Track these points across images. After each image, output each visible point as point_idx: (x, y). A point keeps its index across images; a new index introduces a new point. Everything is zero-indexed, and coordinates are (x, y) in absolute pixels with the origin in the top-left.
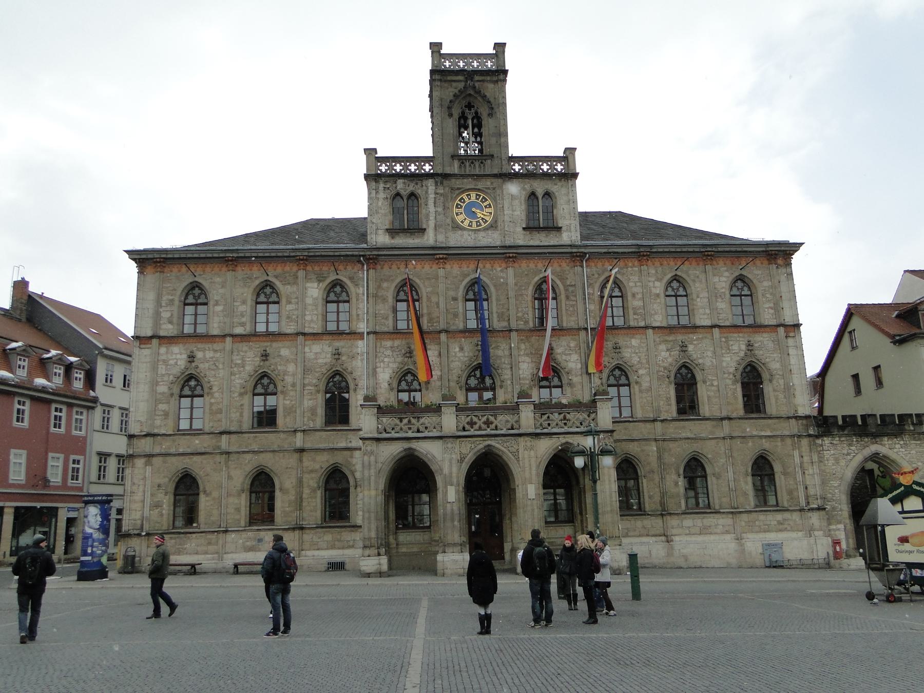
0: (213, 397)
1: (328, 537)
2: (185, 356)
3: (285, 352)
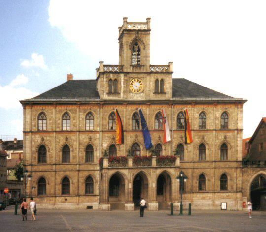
1: (87, 198)
2: (40, 139)
3: (73, 137)
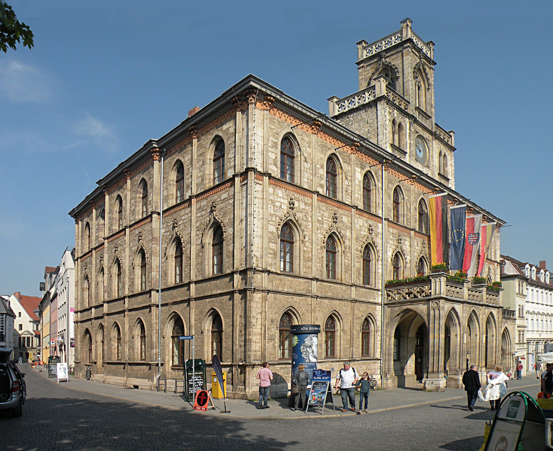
0: (305, 246)
2: (286, 202)
3: (345, 219)
